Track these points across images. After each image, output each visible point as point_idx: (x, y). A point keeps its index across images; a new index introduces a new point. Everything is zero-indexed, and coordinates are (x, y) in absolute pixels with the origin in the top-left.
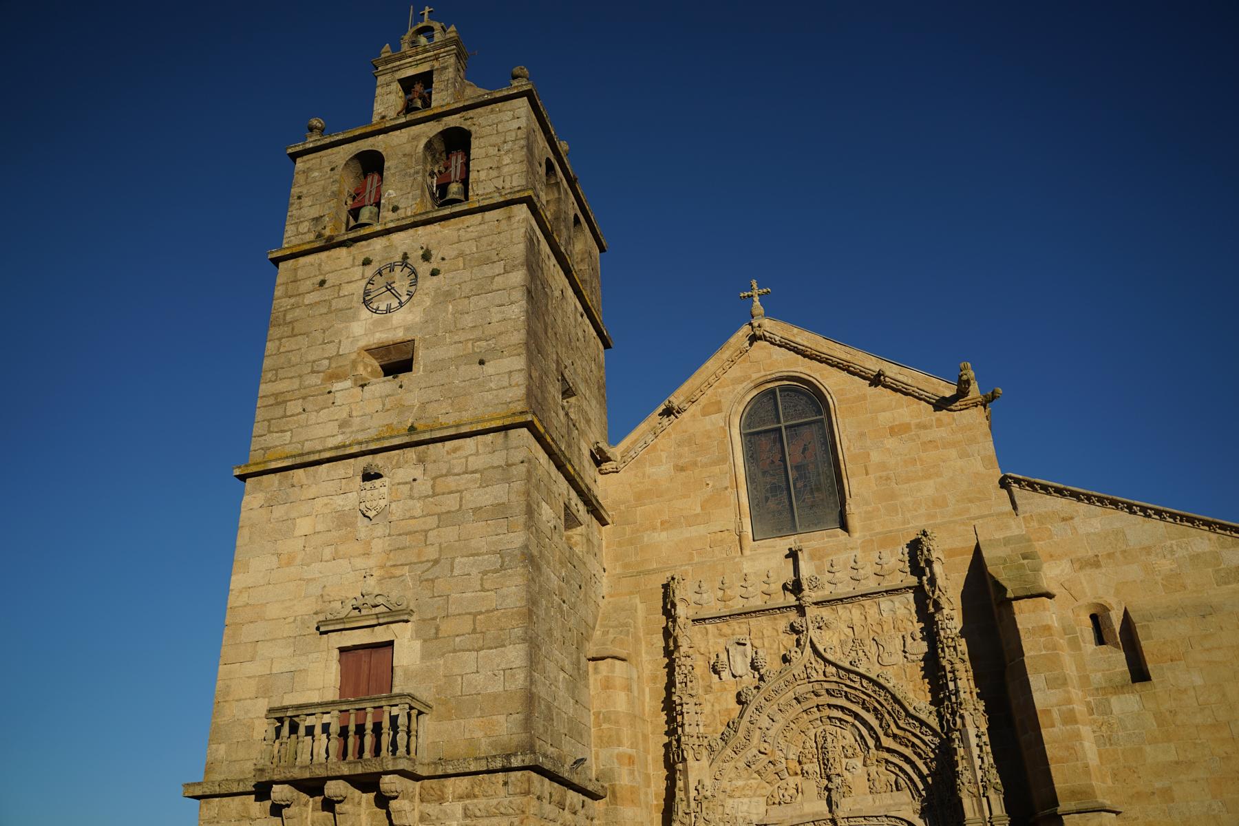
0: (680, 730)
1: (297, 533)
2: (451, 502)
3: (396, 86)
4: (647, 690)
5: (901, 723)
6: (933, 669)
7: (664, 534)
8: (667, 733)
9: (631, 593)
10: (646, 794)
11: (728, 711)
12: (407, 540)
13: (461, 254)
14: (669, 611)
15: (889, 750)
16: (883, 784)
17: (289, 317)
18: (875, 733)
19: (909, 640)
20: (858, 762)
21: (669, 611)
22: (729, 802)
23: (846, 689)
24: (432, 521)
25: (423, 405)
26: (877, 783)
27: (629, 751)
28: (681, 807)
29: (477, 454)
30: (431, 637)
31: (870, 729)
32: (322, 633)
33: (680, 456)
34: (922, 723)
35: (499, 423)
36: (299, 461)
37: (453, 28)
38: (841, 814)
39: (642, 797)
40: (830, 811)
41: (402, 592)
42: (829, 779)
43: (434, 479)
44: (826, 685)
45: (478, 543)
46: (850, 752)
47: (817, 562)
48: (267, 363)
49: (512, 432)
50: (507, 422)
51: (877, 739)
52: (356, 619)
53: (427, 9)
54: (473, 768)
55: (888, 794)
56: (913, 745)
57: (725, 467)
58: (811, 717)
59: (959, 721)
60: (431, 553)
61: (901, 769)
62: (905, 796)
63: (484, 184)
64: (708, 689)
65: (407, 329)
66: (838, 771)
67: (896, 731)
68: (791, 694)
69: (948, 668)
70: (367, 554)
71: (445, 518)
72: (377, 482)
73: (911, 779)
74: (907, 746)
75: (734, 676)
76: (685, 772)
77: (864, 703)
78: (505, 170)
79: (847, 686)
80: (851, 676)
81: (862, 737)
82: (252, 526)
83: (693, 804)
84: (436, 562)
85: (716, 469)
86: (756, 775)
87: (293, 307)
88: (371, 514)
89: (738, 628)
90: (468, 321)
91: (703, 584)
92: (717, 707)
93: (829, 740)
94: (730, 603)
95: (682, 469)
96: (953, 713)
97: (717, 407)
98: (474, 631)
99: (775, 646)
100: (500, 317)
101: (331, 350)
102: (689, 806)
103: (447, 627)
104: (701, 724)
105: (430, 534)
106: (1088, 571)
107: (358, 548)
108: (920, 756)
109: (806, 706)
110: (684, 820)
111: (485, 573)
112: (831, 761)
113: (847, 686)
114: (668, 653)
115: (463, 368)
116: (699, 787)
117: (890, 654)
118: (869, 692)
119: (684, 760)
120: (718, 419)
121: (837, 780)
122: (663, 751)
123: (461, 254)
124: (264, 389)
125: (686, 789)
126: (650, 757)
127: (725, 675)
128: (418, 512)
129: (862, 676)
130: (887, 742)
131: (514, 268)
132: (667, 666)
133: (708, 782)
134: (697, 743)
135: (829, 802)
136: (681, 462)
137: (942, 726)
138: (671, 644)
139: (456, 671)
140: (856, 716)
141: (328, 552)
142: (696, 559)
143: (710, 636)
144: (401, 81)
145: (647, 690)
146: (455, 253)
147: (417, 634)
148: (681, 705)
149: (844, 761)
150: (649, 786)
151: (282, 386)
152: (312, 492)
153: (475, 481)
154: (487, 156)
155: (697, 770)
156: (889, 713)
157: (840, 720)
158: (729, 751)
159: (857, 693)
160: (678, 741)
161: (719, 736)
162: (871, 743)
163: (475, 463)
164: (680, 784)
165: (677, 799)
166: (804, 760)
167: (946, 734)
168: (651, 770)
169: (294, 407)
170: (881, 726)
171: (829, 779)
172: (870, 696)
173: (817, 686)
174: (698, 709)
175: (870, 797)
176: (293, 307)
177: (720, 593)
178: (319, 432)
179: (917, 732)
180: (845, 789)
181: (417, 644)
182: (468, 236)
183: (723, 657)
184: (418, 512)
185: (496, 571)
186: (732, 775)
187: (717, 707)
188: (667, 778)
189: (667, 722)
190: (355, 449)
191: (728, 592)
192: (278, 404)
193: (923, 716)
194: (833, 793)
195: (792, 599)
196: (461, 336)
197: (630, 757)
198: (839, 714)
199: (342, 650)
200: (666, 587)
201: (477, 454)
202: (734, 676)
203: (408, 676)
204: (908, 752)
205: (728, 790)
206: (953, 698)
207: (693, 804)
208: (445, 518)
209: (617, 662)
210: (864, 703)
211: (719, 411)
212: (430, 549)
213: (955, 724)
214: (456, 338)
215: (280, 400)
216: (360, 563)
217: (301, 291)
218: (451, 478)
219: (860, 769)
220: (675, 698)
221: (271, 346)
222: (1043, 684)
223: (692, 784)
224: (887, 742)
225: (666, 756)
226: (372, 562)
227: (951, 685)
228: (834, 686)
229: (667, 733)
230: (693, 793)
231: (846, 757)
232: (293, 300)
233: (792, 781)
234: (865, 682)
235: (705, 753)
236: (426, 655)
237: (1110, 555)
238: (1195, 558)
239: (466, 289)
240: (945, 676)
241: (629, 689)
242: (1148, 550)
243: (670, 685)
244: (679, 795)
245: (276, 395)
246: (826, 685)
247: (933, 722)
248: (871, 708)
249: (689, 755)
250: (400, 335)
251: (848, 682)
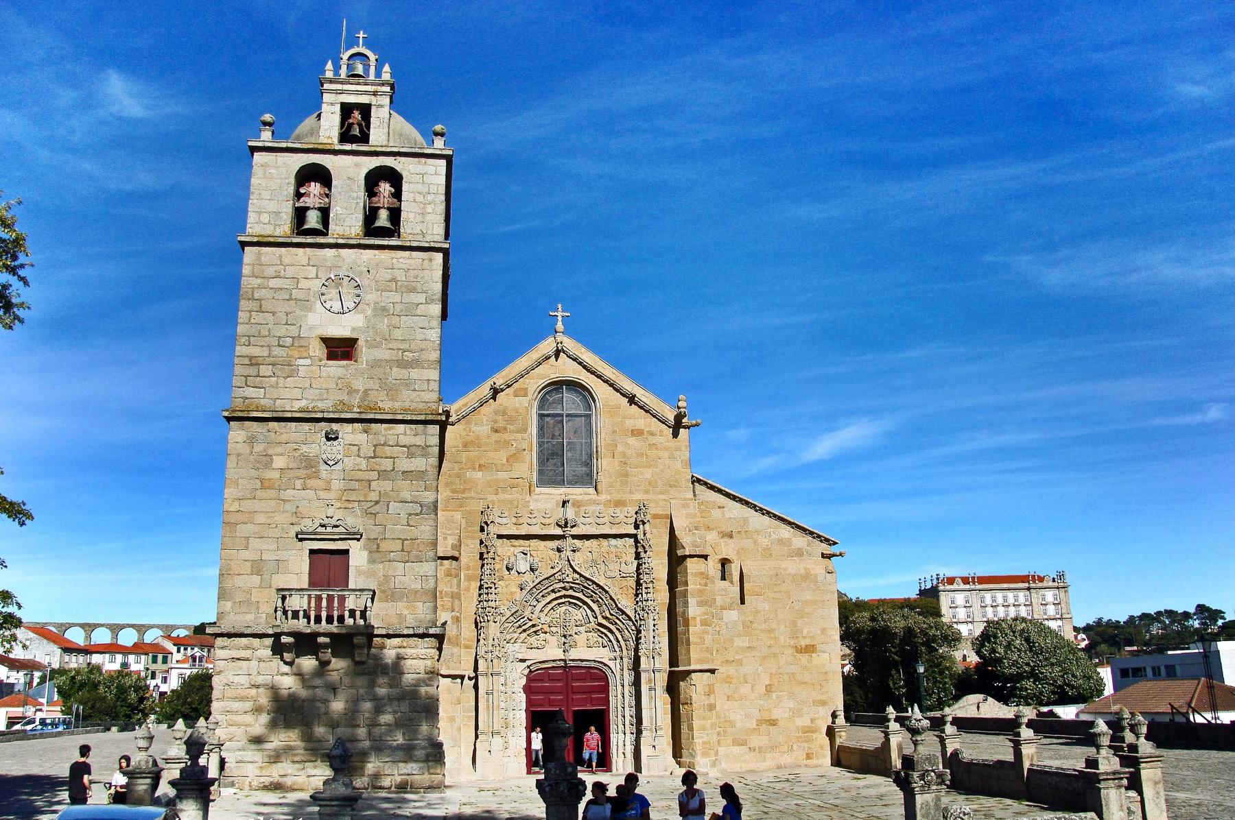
1: (274, 466)
2: (387, 464)
3: (338, 107)
7: (480, 474)
12: (355, 485)
13: (394, 280)
17: (256, 296)
24: (375, 475)
25: (366, 391)
29: (405, 434)
30: (376, 551)
32: (301, 540)
33: (496, 422)
34: (624, 613)
35: (422, 418)
36: (275, 415)
37: (387, 68)
41: (353, 521)
43: (375, 446)
45: (406, 495)
48: (241, 329)
49: (430, 427)
50: (430, 417)
52: (320, 534)
53: (361, 35)
54: (405, 632)
57: (525, 436)
60: (374, 496)
63: (411, 227)
65: (353, 329)
70: (328, 490)
71: (383, 475)
72: (335, 443)
78: (428, 217)
82: (239, 455)
84: (377, 503)
85: (519, 436)
87: (260, 287)
88: (331, 463)
90: (398, 334)
95: (496, 431)
97: (523, 392)
98: (403, 550)
100: (423, 337)
101: (294, 331)
103: (385, 546)
105: (373, 483)
106: (726, 539)
107: (320, 484)
111: (410, 515)
115: (395, 369)
120: (524, 401)
123: (394, 280)
124: (240, 350)
128: (364, 467)
129: (594, 582)
131: (432, 301)
136: (496, 426)
139: (391, 573)
141: (298, 484)
144: (342, 104)
146: (389, 277)
147: (365, 547)
151: (255, 351)
152: (285, 437)
153: (403, 453)
154: (414, 201)
163: (404, 440)
169: (265, 370)
176: (260, 287)
177: (514, 520)
178: (287, 394)
181: (365, 553)
182: (400, 266)
183: (512, 559)
184: (364, 467)
185: (417, 514)
190: (319, 415)
192: (252, 365)
196: (394, 345)
199: (312, 552)
201: (405, 434)
203: (360, 572)
208: (383, 475)
211: (525, 395)
212: (373, 494)
214: (390, 346)
215: (254, 362)
216: (322, 494)
217: (265, 274)
218: (387, 448)
221: (242, 316)
226: (332, 495)
232: (259, 281)
236: (371, 561)
237: (739, 532)
238: (781, 541)
239: (398, 308)
242: (758, 532)
245: (251, 358)
250: (346, 333)
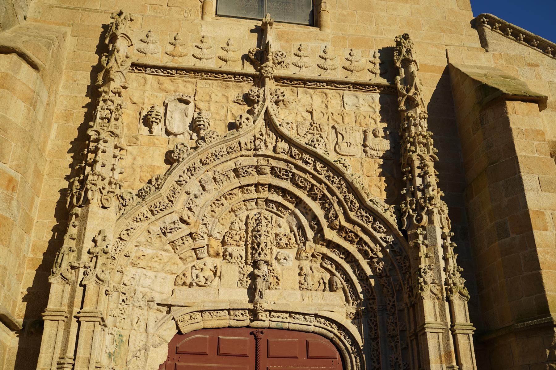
0: (88, 170)
4: (55, 126)
5: (352, 215)
6: (396, 168)
8: (68, 178)
9: (63, 24)
10: (22, 239)
11: (152, 168)
14: (105, 49)
15: (330, 244)
16: (316, 280)
18: (318, 223)
19: (370, 136)
20: (291, 253)
21: (105, 49)
22: (130, 271)
23: (294, 170)
26: (309, 279)
27: (12, 173)
28: (67, 259)
31: (314, 218)
34: (377, 217)
38: (266, 306)
39: (15, 237)
40: (251, 301)
42: (255, 265)
44: (273, 163)
46: (284, 241)
47: (284, 44)
51: (319, 231)
55: (320, 293)
56: (361, 241)
58: (247, 197)
59: (425, 218)
61: (339, 267)
62: (338, 297)
64: (134, 140)
66: (268, 258)
67: (344, 223)
68: (231, 165)
69: (417, 163)
73: (348, 280)
74: (351, 242)
75: (168, 133)
76: (84, 219)
77: (312, 189)
79: (297, 167)
80: (306, 156)
81: (300, 227)
83: (85, 257)
86: (169, 247)
89: (183, 86)
91: (152, 34)
92: (139, 162)
93: (264, 221)
94: (180, 59)
96: (419, 208)
99: (223, 112)
102: (79, 258)
104: (118, 170)
108: (365, 254)
109: (244, 181)
110: (68, 275)
112: (263, 245)
113: (297, 167)
114: (94, 92)
116: (99, 238)
117: (349, 144)
118: (322, 177)
119: (87, 202)
121: (265, 268)
122: (58, 196)
125: (80, 239)
126: (38, 201)
127: (158, 129)
129: (318, 158)
130: (330, 235)
132: (87, 106)
133: (112, 239)
134: (108, 188)
135: (252, 291)
137: (400, 223)
138: (100, 77)
140: (299, 202)
142: (148, 12)
143: (148, 87)
145: (55, 126)
148: (97, 141)
149: (276, 250)
150: (27, 232)
155: (100, 219)
156: (340, 203)
157: (279, 205)
158: (144, 209)
159: (308, 177)
160: (83, 183)
161: (135, 192)
162: (310, 234)
164: (73, 231)
165: (65, 248)
166: (230, 241)
167: (404, 232)
168: (35, 215)
170: (326, 217)
171: (255, 265)
172: (320, 181)
173: (262, 161)
174: (117, 152)
175: (299, 293)
177: (170, 48)
179: (369, 227)
180: (271, 280)
186: (142, 239)
187: (139, 162)
188: (55, 229)
189: (71, 166)
191: (180, 49)
193: (380, 210)
194: (259, 281)
195: (250, 69)
197: (11, 180)
198: (279, 199)
200: (106, 28)
202: (168, 133)
204: (352, 249)
205: (132, 256)
206: (419, 194)
207: (85, 257)
209: (25, 66)
210: (312, 189)
213: (420, 220)
219: (292, 264)
220: (91, 132)
222: (536, 185)
223: (89, 235)
224: (330, 235)
225: (61, 204)
227: (418, 181)
228: (282, 165)
229: (68, 178)
230: (88, 244)
231: (278, 246)
233: (211, 262)
234: (319, 166)
235: (114, 203)
240: (412, 172)
241: (33, 104)
243: (90, 116)
244: (68, 243)
246: (273, 163)
247: (391, 218)
248: (319, 195)
249: (95, 198)
251: (300, 163)
